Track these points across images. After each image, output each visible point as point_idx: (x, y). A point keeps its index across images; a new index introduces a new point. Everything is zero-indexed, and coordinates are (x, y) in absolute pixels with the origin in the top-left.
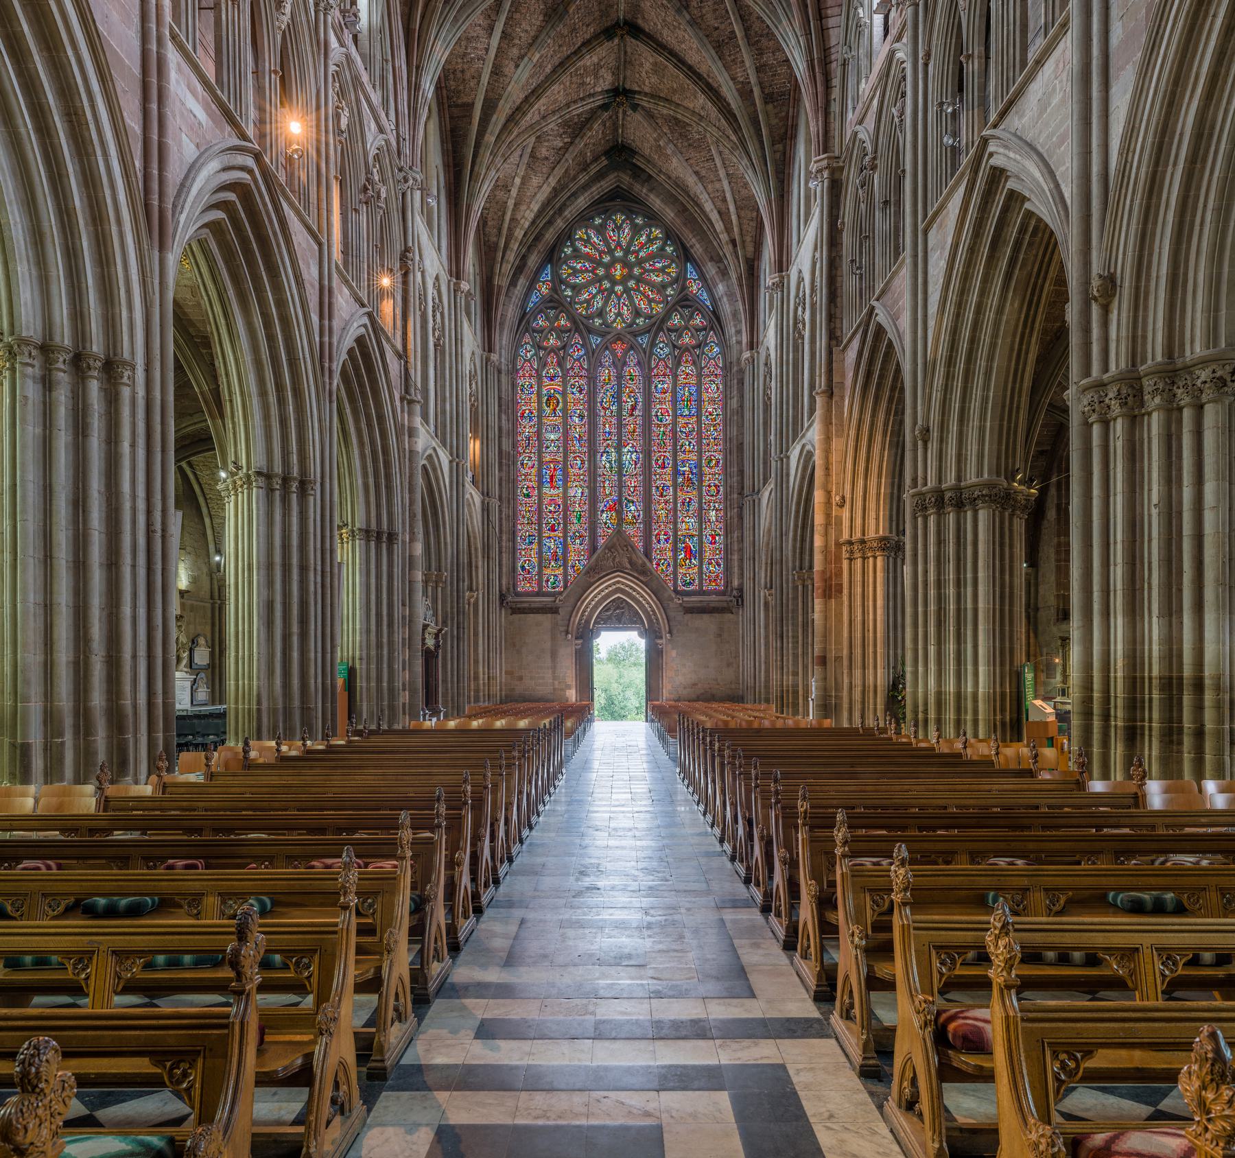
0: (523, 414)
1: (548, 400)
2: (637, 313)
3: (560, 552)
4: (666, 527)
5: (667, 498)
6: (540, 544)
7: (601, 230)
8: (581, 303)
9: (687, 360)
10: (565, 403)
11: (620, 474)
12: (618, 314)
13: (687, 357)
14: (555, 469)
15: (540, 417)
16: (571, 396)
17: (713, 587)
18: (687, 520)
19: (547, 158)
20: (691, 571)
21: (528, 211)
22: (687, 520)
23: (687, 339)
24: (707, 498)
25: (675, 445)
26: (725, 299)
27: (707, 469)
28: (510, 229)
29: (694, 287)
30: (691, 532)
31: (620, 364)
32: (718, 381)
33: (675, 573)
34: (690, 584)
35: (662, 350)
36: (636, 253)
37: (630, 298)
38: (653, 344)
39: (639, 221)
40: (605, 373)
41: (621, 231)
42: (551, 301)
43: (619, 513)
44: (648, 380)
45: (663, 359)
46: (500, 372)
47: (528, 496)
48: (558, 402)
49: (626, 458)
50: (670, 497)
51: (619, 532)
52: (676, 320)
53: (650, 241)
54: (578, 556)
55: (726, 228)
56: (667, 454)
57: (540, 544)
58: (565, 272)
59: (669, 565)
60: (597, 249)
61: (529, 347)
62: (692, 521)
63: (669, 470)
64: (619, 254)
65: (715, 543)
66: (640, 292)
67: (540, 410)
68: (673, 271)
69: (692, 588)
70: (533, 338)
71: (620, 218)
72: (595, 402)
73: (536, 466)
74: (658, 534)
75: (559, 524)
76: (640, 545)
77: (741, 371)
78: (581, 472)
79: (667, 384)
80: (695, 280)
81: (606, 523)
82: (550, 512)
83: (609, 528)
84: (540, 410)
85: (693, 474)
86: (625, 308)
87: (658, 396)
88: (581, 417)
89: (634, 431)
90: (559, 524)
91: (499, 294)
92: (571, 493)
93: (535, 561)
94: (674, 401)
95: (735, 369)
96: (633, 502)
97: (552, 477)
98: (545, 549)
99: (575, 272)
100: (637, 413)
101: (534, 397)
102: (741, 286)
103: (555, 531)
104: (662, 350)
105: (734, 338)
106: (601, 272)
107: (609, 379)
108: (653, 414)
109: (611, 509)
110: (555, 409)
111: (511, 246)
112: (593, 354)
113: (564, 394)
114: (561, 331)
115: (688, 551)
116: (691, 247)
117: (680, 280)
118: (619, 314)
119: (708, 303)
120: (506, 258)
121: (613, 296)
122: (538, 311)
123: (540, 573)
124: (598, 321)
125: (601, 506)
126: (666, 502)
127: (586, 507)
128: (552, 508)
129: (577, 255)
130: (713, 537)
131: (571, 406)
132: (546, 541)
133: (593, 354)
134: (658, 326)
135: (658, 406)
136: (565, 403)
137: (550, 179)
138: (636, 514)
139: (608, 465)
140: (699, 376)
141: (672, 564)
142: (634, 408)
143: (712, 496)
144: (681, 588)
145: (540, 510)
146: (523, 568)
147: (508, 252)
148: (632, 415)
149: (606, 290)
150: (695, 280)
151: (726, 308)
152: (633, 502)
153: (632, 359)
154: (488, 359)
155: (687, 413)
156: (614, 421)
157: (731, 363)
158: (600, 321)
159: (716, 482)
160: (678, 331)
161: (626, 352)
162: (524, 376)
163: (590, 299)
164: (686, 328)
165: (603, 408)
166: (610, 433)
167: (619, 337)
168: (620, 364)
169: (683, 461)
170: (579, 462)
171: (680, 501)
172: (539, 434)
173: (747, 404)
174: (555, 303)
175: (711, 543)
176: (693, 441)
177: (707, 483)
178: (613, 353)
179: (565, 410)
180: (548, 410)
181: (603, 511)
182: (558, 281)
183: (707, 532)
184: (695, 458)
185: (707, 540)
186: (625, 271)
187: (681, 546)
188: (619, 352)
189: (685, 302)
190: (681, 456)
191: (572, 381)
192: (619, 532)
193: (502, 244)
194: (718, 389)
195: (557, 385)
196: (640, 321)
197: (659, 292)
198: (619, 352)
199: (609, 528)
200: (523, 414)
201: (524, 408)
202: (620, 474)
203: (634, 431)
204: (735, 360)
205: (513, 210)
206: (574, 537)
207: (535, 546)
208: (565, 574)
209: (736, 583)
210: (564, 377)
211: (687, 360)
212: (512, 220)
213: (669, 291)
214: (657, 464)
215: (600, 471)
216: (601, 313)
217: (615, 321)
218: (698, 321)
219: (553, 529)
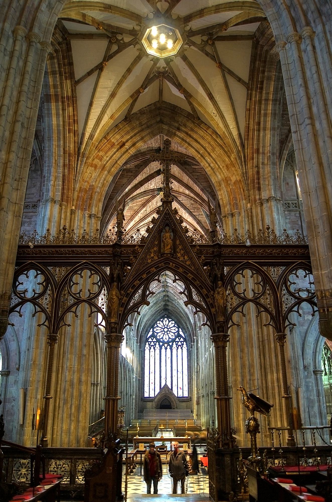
2: (169, 338)
12: (166, 338)
13: (180, 347)
23: (180, 343)
29: (181, 333)
31: (166, 349)
35: (174, 345)
38: (173, 344)
39: (170, 320)
40: (163, 350)
41: (166, 321)
52: (177, 340)
54: (158, 390)
58: (155, 330)
68: (177, 330)
71: (166, 319)
77: (190, 351)
104: (174, 345)
114: (154, 342)
117: (178, 331)
122: (149, 337)
129: (157, 326)
134: (173, 341)
144: (179, 396)
151: (187, 339)
153: (168, 347)
161: (167, 346)
163: (160, 336)
167: (166, 343)
168: (166, 349)
173: (191, 359)
174: (153, 336)
182: (153, 331)
189: (179, 336)
196: (170, 340)
209: (190, 396)
216: (162, 338)
218: (182, 340)
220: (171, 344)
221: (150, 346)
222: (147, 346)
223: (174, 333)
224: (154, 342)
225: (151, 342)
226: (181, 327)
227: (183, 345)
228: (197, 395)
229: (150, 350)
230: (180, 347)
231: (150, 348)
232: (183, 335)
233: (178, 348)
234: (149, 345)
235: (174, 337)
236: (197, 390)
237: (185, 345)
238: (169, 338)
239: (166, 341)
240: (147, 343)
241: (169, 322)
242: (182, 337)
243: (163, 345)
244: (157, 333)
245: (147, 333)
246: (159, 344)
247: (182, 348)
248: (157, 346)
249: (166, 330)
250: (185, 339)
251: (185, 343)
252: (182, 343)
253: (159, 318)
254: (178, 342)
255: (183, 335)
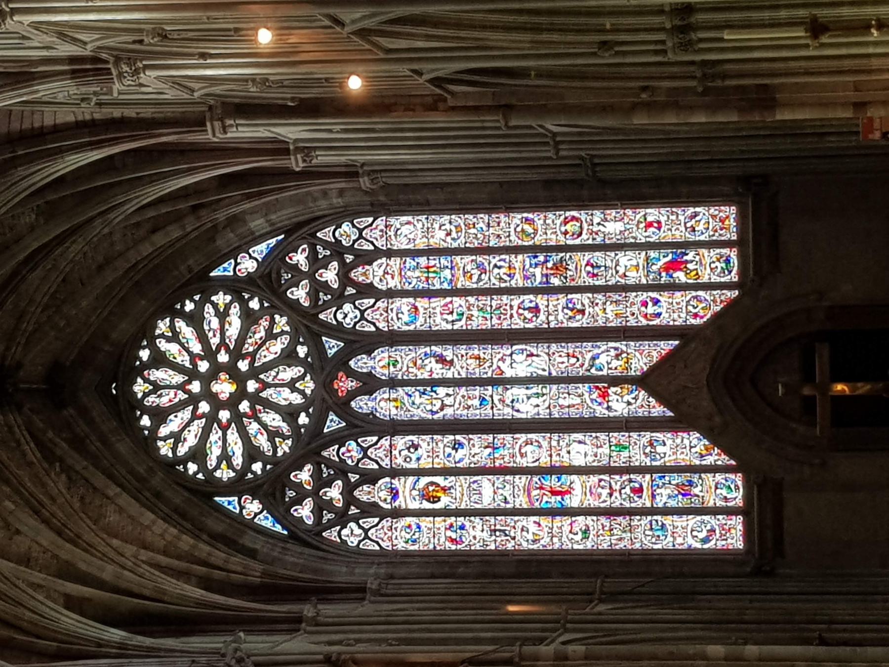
0: (453, 541)
1: (428, 500)
2: (288, 357)
3: (676, 479)
4: (633, 304)
5: (586, 302)
6: (666, 511)
7: (160, 415)
8: (275, 448)
9: (364, 274)
10: (433, 472)
11: (549, 380)
13: (357, 274)
14: (541, 488)
15: (458, 513)
16: (422, 461)
17: (732, 222)
18: (621, 270)
19: (82, 498)
20: (708, 260)
21: (154, 528)
22: (621, 270)
23: (330, 275)
24: (584, 236)
25: (500, 292)
26: (273, 217)
27: (538, 237)
28: (179, 558)
29: (248, 265)
30: (641, 262)
32: (395, 221)
33: (709, 287)
34: (728, 261)
35: (348, 315)
36: (193, 357)
37: (268, 367)
38: (337, 331)
39: (145, 354)
42: (273, 495)
43: (615, 381)
44: (394, 339)
45: (362, 312)
46: (392, 577)
47: (586, 532)
48: (432, 483)
49: (522, 370)
50: (585, 298)
51: (643, 381)
52: (300, 294)
53: (175, 337)
55: (175, 221)
56: (516, 303)
57: (666, 511)
59: (696, 297)
60: (188, 424)
61: (345, 532)
62: (625, 259)
63: (541, 301)
64: (195, 387)
65: (659, 222)
66: (256, 351)
67: (446, 513)
68: (221, 299)
69: (734, 260)
70: (330, 525)
71: (140, 387)
72: (433, 422)
73: (536, 518)
74: (645, 316)
75: (630, 481)
76: (666, 346)
78: (545, 444)
79: (403, 304)
80: (237, 264)
81: (629, 403)
82: (611, 495)
83: (636, 398)
84: (446, 513)
85: (546, 261)
86: (280, 376)
87: (421, 320)
88: (457, 446)
89: (478, 358)
90: (630, 481)
91: (275, 576)
92: (579, 461)
93: (693, 521)
94: (429, 294)
95: (382, 198)
96: (594, 358)
97: (554, 493)
98: (672, 503)
99: (225, 457)
100: (448, 354)
101: (425, 522)
102: (260, 194)
103: (641, 486)
104: (348, 315)
105: (335, 201)
106: (224, 415)
107: (395, 400)
108: (449, 327)
109: (604, 395)
110: (444, 489)
111: (203, 555)
112: (357, 426)
113: (419, 473)
114: (321, 483)
115: (674, 266)
116: (190, 271)
118: (292, 385)
119: (273, 242)
120: (220, 563)
121: (264, 394)
123: (714, 511)
124: (303, 419)
125: (600, 411)
126: (593, 304)
127: (602, 436)
128: (605, 492)
129: (198, 454)
130: (650, 225)
131: (439, 463)
132: (660, 503)
133: (357, 426)
135: (438, 319)
136: (433, 472)
137: (111, 493)
138: (613, 353)
139: (534, 401)
140: (390, 253)
141: (694, 293)
142: (441, 360)
143: (581, 227)
144: (734, 277)
145: (611, 513)
146: (705, 541)
147: (213, 560)
148: (451, 362)
149: (252, 408)
150: (237, 264)
151: (285, 215)
152: (594, 358)
153: (360, 363)
154: (377, 593)
155: (447, 273)
156: (463, 391)
157: (372, 205)
158: (303, 415)
159: (558, 222)
160: (317, 287)
161: (352, 374)
162: (390, 539)
164: (311, 276)
165: (442, 409)
166: (483, 400)
167: (325, 384)
169: (526, 278)
170: (529, 448)
171: (590, 281)
172: (482, 513)
175: (659, 228)
176: (494, 261)
177: (561, 238)
178: (353, 394)
179: (445, 472)
180: (444, 501)
181: (609, 408)
183: (641, 236)
184: (520, 257)
185: (653, 235)
186: (223, 376)
187: (664, 278)
188: (351, 384)
190: (518, 281)
191: (400, 461)
192: (643, 381)
193: (202, 570)
194: (408, 223)
195: (404, 485)
196: (302, 351)
197: (256, 322)
198: (351, 384)
199: (636, 398)
200: (453, 541)
201: (443, 539)
202: (549, 380)
203: (478, 358)
204: (367, 199)
205: (153, 551)
206: (652, 455)
207: (668, 520)
208: (713, 469)
210: (395, 473)
211: (364, 274)
212: (165, 553)
213: (254, 304)
214: (531, 320)
215: (544, 414)
216: (290, 413)
217: (302, 393)
218: (300, 258)
219: (639, 491)
220: (332, 346)
221: (353, 510)
222: (351, 535)
223: (249, 318)
224: (321, 483)
225: (321, 507)
226: (194, 262)
227: (337, 250)
228: (691, 108)
229: (382, 514)
230: (357, 274)
231: (371, 509)
232: (261, 250)
233: (367, 290)
234: (342, 519)
235: (282, 322)
236: (650, 107)
237: (346, 232)
238: (288, 357)
239: (308, 386)
240: (332, 535)
241: (160, 360)
242: (277, 257)
243: (343, 407)
244: (252, 453)
245: (249, 540)
246: (339, 438)
247: (367, 258)
248: (351, 451)
249: (224, 388)
250: (299, 225)
251: (326, 234)
252: (322, 252)
253: (123, 447)
254: (317, 287)
255: (261, 250)
